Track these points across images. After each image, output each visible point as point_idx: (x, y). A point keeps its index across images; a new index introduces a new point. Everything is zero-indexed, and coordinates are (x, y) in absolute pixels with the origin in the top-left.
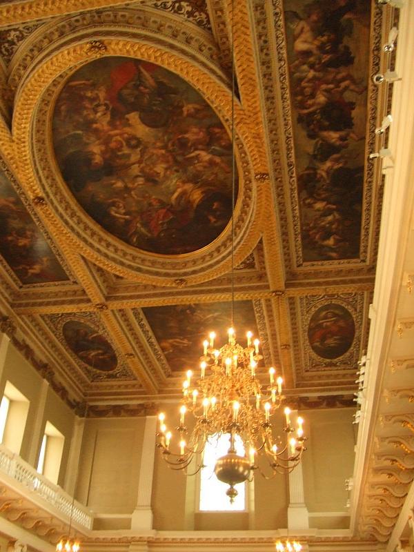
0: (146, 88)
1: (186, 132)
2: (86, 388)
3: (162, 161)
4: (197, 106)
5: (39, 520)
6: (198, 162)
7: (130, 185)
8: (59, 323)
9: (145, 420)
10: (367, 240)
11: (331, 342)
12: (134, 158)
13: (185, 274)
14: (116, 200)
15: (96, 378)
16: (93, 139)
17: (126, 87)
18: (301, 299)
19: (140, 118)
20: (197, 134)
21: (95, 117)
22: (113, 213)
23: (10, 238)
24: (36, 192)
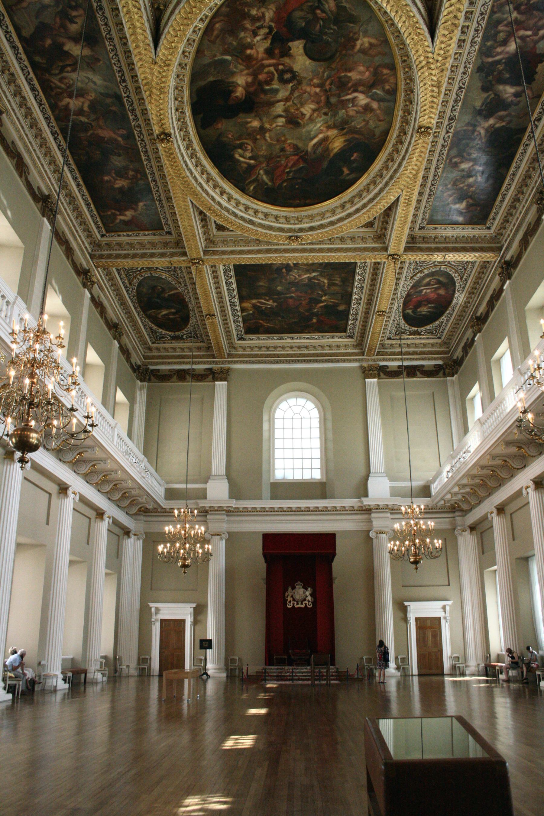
0: (323, 11)
1: (350, 70)
2: (146, 351)
3: (313, 101)
4: (373, 41)
5: (126, 490)
6: (352, 106)
7: (267, 126)
8: (135, 277)
9: (215, 385)
10: (500, 207)
11: (424, 310)
12: (282, 95)
13: (301, 230)
14: (245, 141)
15: (158, 338)
16: (241, 67)
18: (410, 263)
19: (305, 48)
20: (361, 73)
21: (252, 41)
22: (237, 156)
23: (106, 178)
24: (164, 127)
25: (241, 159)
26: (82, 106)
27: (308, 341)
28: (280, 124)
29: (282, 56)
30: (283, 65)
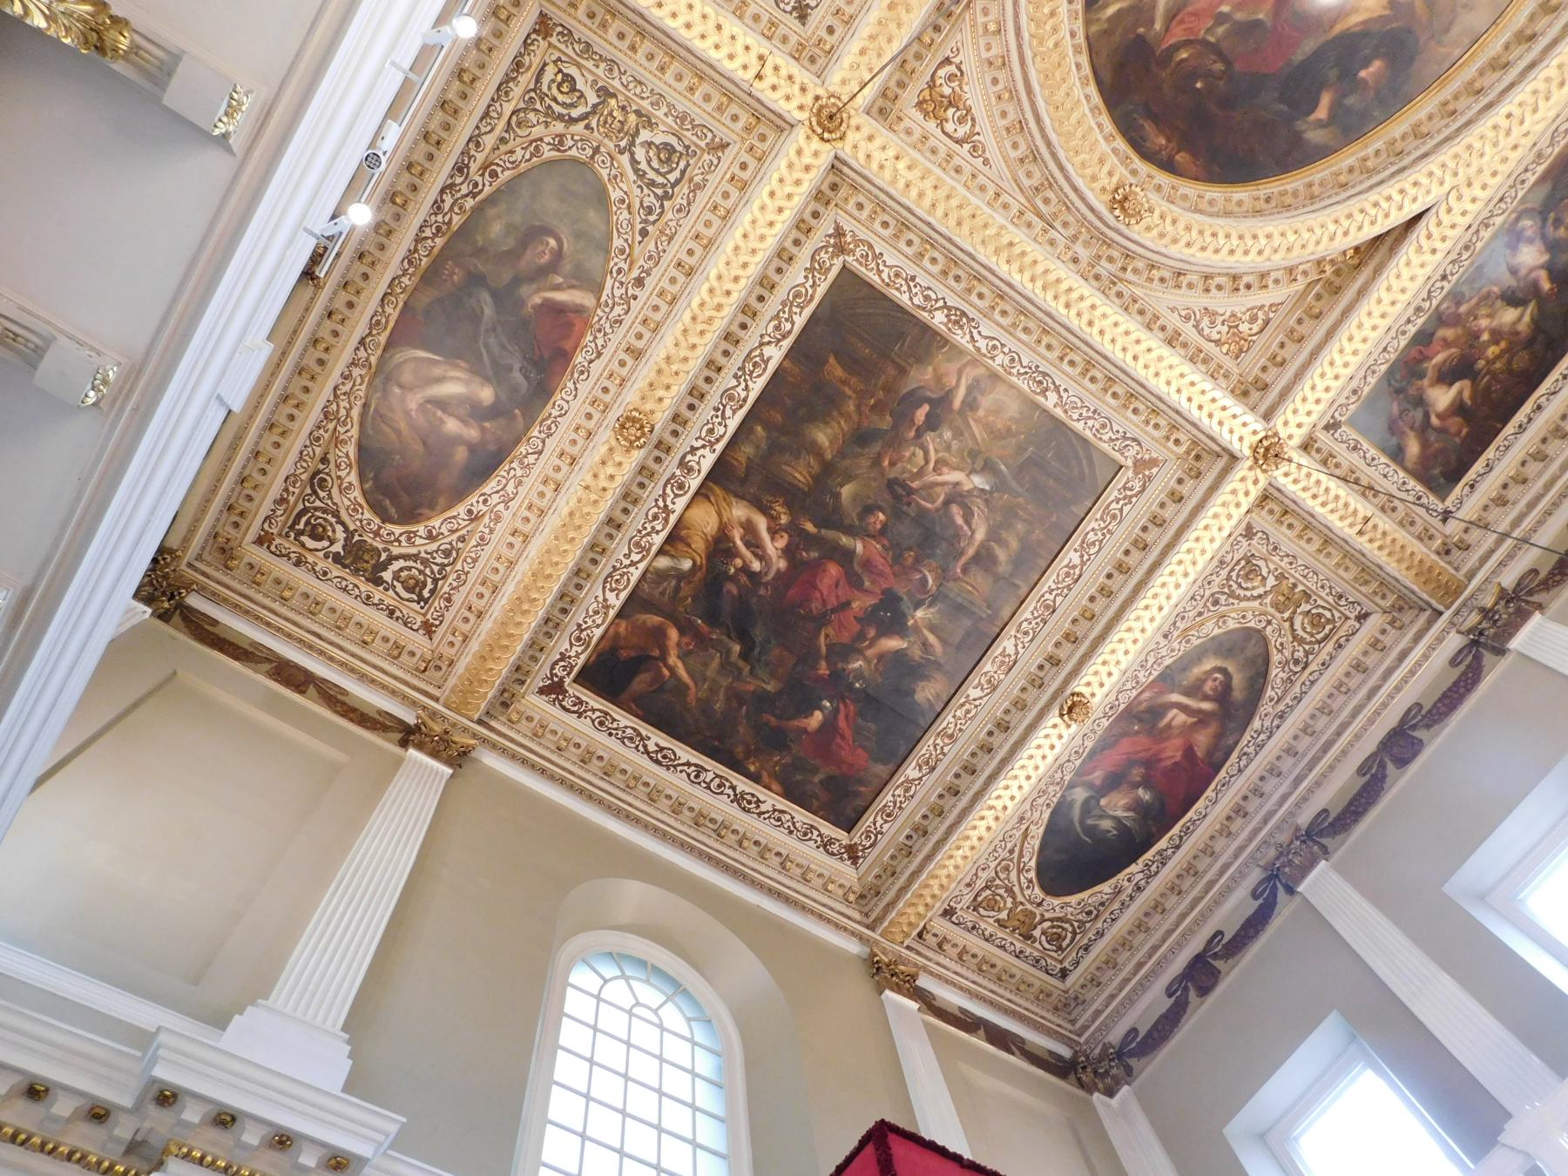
27: (734, 811)
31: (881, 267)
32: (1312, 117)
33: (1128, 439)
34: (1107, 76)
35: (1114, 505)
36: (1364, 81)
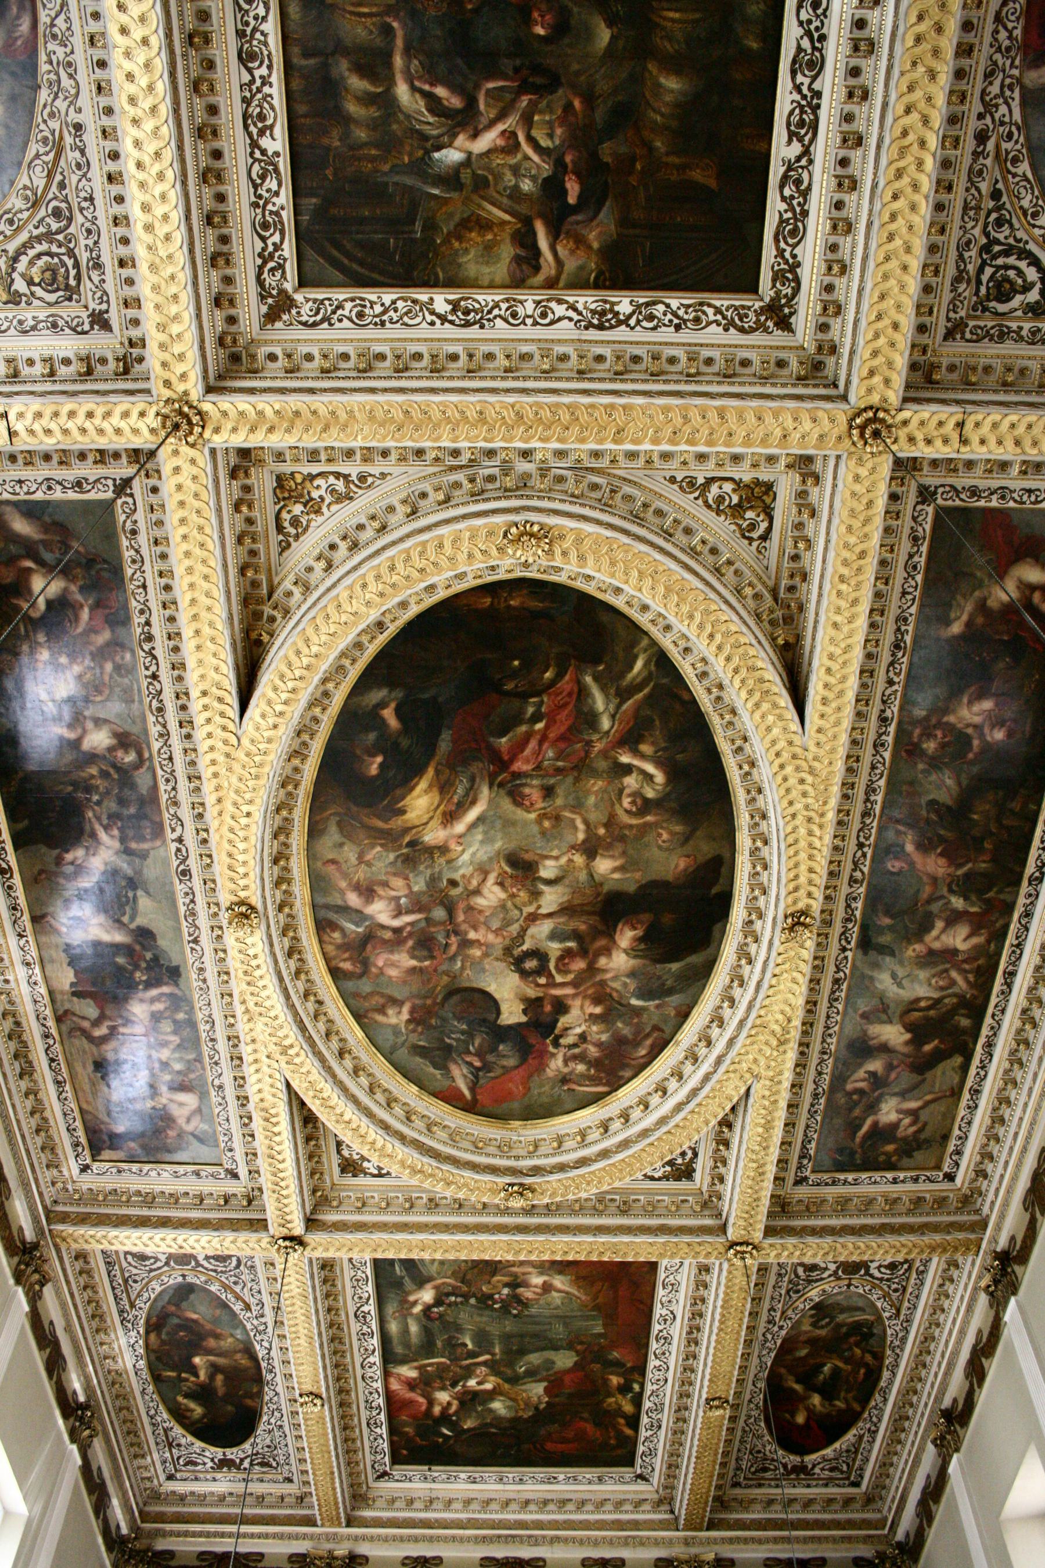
1: (413, 970)
3: (480, 912)
4: (380, 1018)
6: (399, 898)
7: (579, 859)
12: (545, 927)
14: (634, 821)
16: (616, 985)
17: (506, 1070)
19: (498, 1012)
20: (393, 965)
22: (660, 778)
25: (650, 768)
26: (943, 931)
28: (549, 863)
29: (539, 1000)
30: (538, 985)
31: (719, 317)
32: (393, 705)
33: (322, 321)
34: (605, 618)
35: (276, 238)
36: (374, 755)
